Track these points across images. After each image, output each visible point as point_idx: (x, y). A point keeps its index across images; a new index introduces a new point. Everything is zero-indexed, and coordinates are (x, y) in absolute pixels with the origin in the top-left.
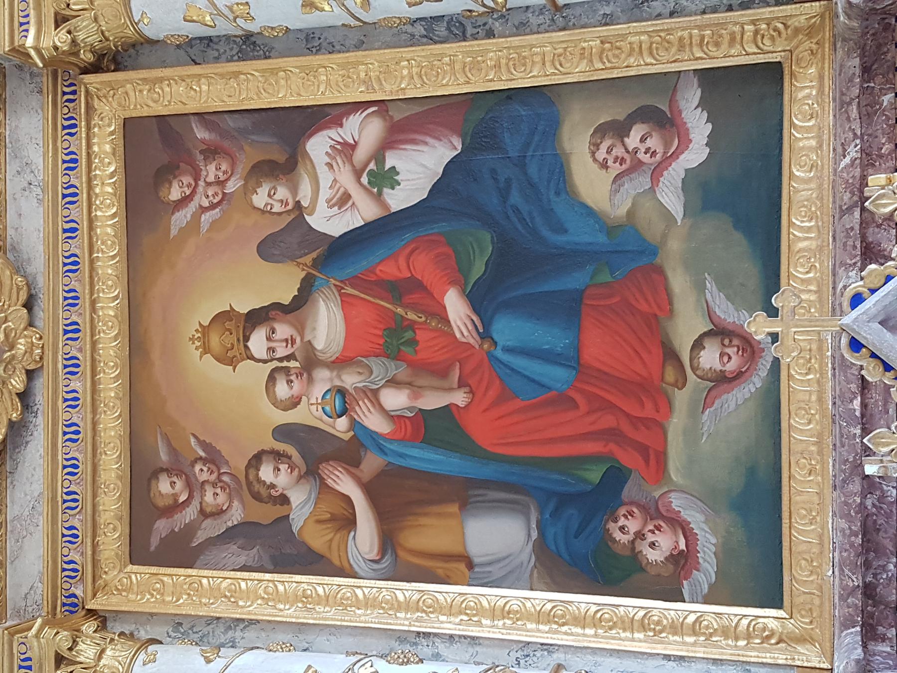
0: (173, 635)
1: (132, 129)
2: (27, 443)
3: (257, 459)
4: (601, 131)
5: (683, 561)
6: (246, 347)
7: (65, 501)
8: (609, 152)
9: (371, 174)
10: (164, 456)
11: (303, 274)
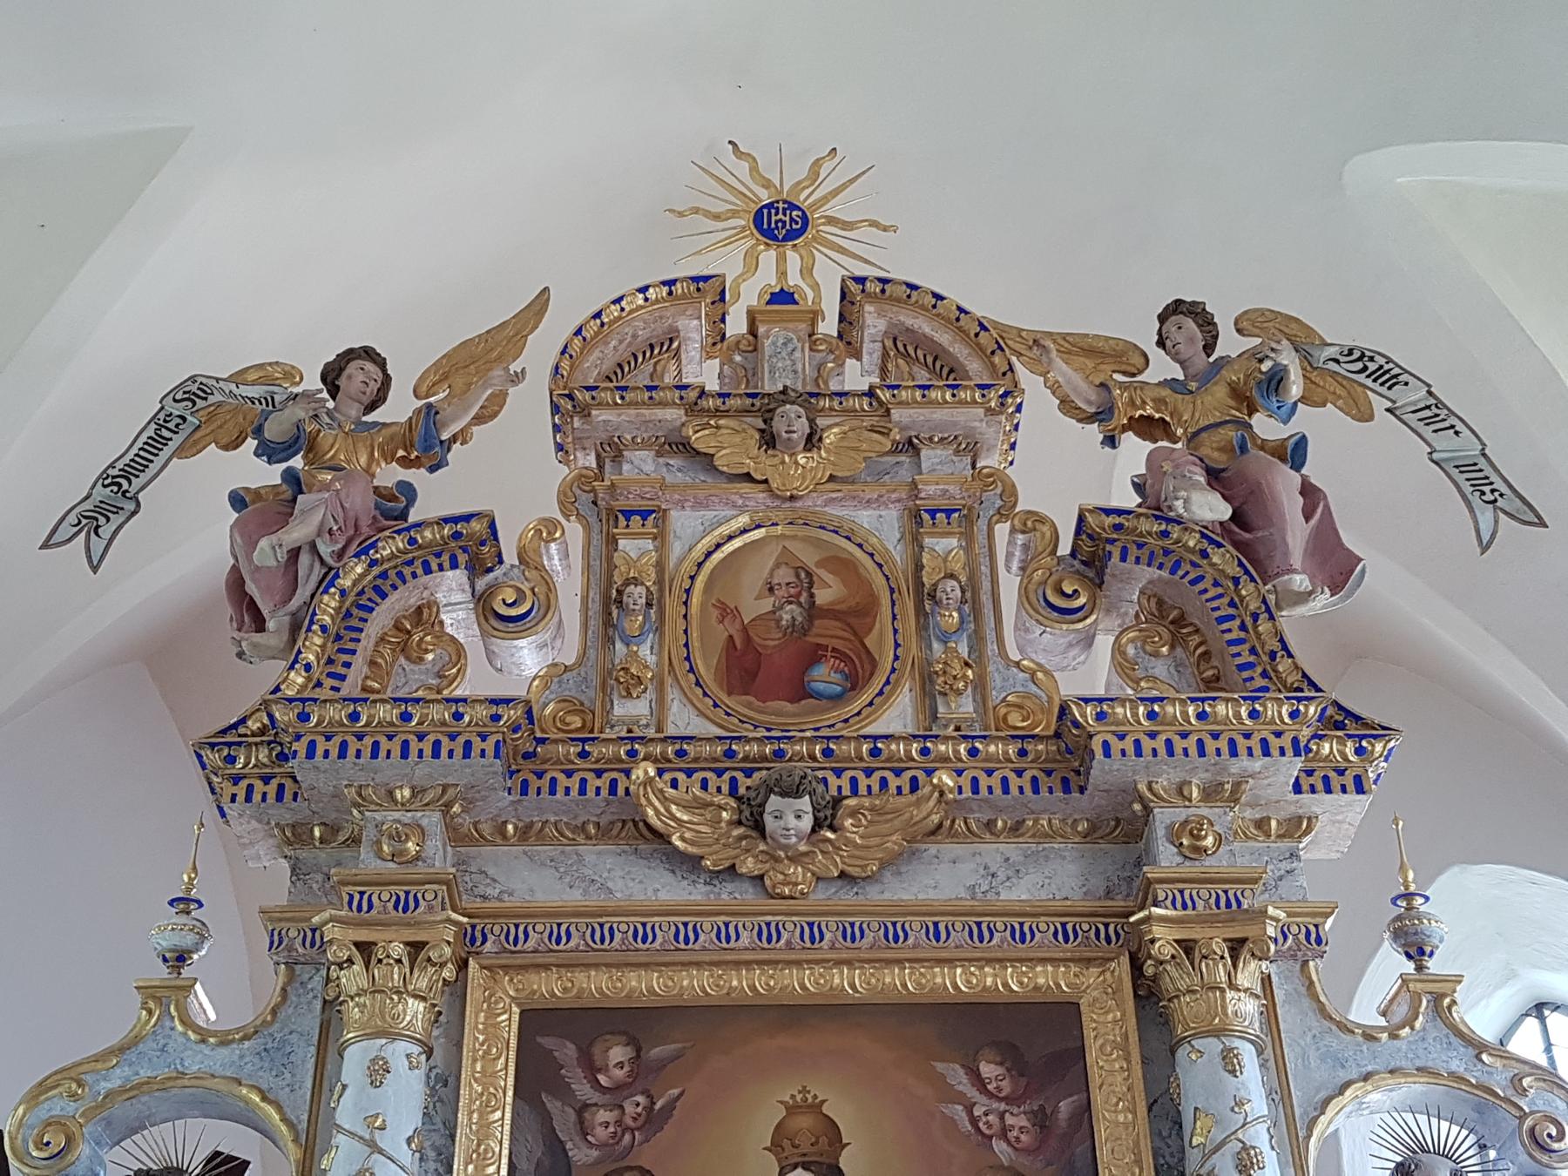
0: (433, 1075)
2: (673, 872)
6: (795, 1167)
7: (601, 926)
10: (656, 1052)
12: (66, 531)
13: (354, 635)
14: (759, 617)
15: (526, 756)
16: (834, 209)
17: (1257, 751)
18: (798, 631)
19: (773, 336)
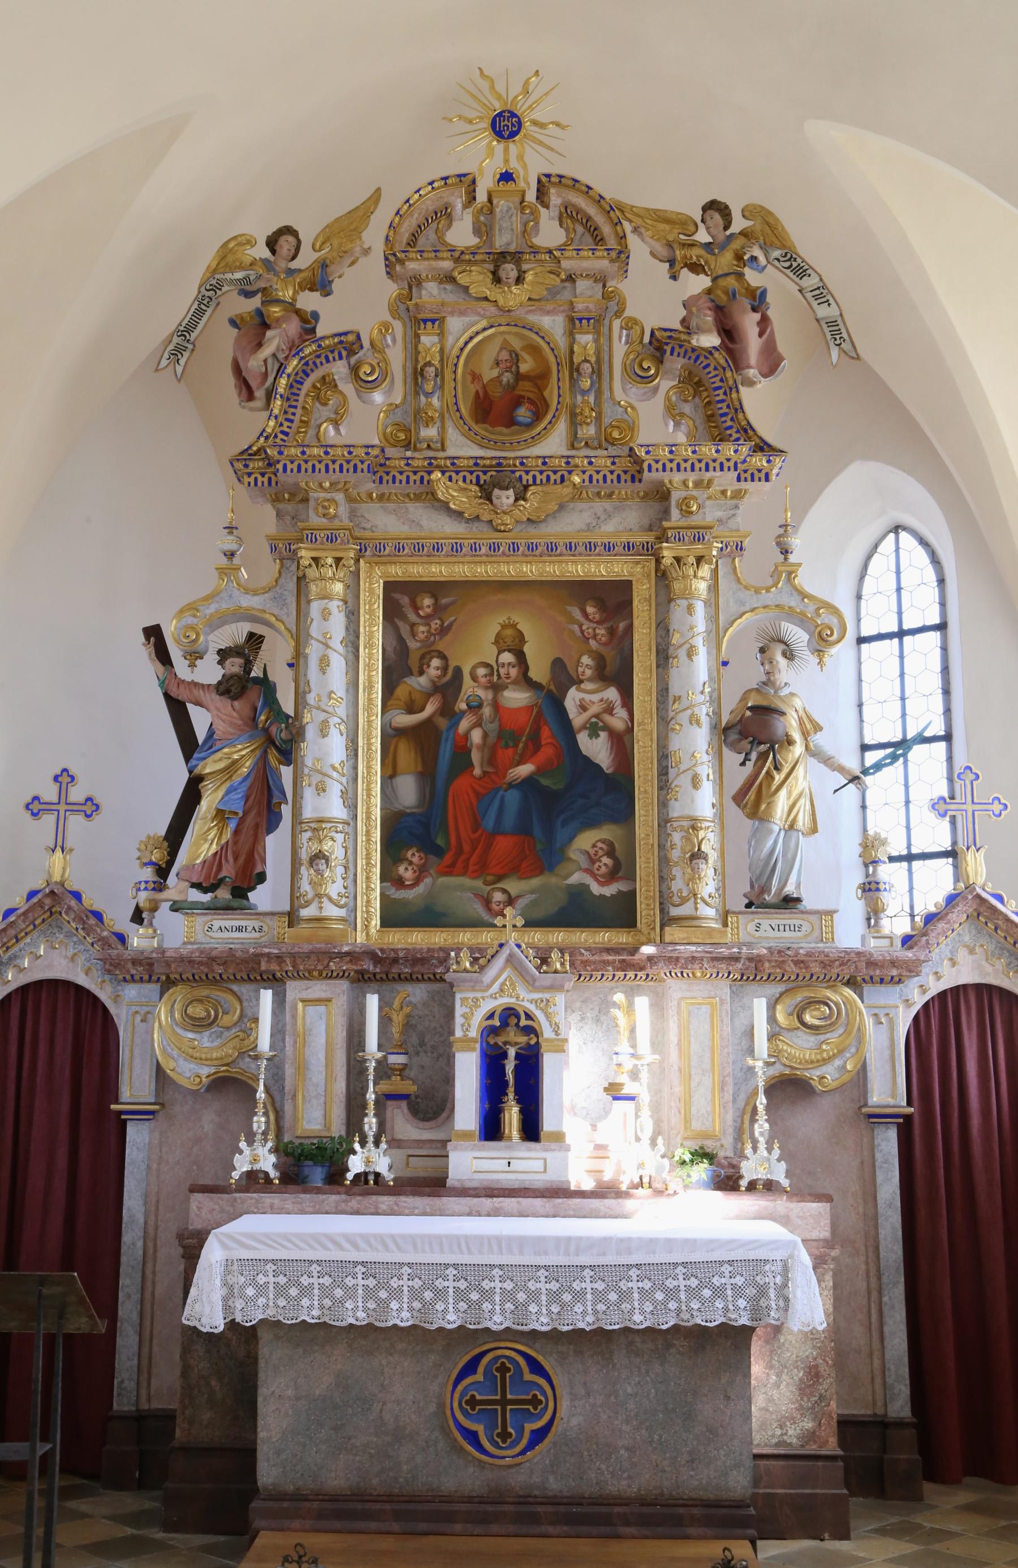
3: (443, 657)
5: (399, 883)
6: (504, 651)
8: (601, 848)
9: (596, 723)
10: (444, 601)
11: (544, 684)
12: (164, 362)
13: (296, 397)
14: (492, 380)
15: (381, 465)
16: (536, 115)
17: (718, 468)
18: (511, 388)
19: (501, 205)
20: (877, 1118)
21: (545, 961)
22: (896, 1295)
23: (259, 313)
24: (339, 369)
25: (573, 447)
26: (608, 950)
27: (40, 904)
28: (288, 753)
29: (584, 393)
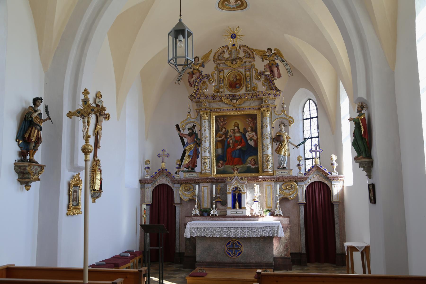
1: (256, 115)
3: (225, 128)
4: (254, 159)
5: (219, 166)
19: (233, 50)
20: (300, 204)
21: (242, 179)
22: (303, 233)
23: (192, 72)
24: (206, 80)
25: (246, 91)
26: (253, 177)
27: (161, 171)
28: (200, 145)
29: (248, 82)
